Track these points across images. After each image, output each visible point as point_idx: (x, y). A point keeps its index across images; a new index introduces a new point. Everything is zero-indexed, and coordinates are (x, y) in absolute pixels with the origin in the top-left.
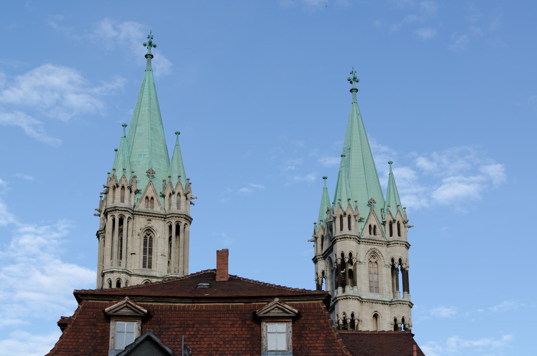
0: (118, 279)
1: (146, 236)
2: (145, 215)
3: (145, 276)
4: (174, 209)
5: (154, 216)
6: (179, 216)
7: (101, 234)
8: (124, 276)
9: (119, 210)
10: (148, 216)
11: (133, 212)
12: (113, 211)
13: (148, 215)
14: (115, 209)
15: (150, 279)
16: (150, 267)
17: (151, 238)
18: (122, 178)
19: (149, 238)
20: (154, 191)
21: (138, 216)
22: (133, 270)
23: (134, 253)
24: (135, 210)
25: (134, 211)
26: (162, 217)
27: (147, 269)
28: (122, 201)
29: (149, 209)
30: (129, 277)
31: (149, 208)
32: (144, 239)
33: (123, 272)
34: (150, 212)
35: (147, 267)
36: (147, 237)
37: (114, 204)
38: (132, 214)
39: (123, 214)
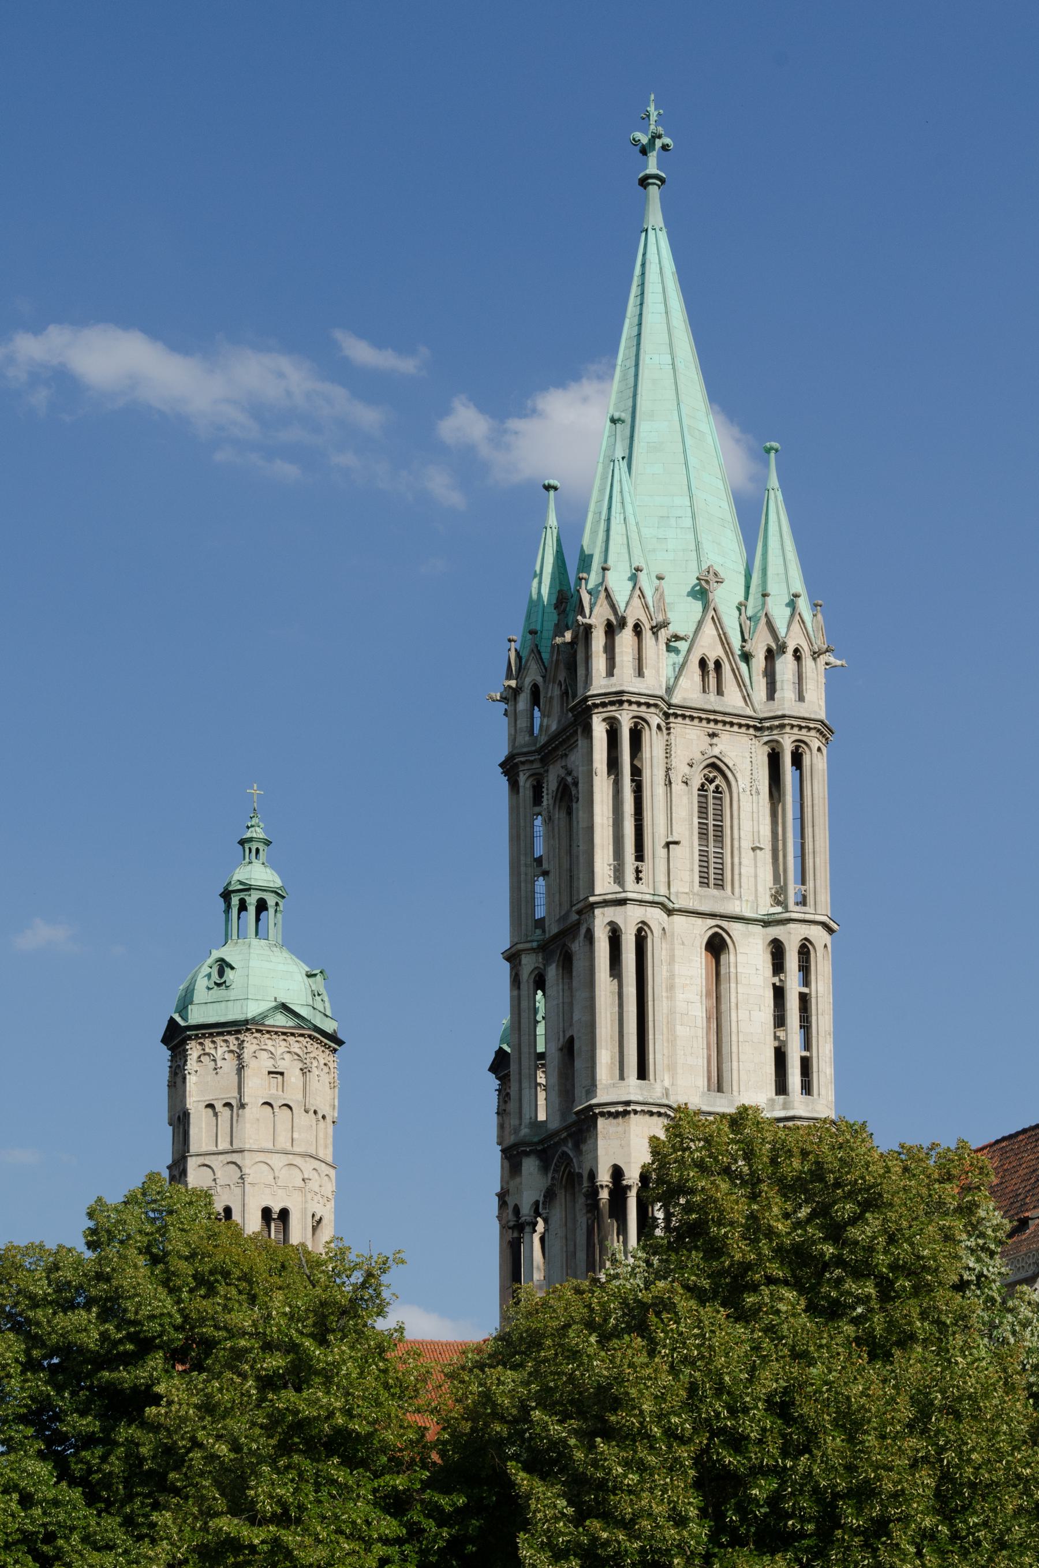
0: (640, 925)
1: (703, 785)
2: (701, 719)
3: (713, 916)
4: (786, 701)
5: (725, 723)
6: (804, 723)
7: (523, 763)
8: (658, 917)
9: (630, 703)
10: (709, 721)
11: (669, 709)
12: (612, 703)
13: (712, 717)
14: (618, 698)
15: (726, 923)
16: (720, 885)
17: (717, 790)
18: (631, 596)
19: (714, 792)
20: (724, 640)
21: (680, 720)
22: (677, 893)
23: (677, 840)
24: (675, 701)
25: (670, 705)
26: (748, 727)
27: (713, 891)
28: (640, 673)
29: (712, 696)
30: (665, 916)
31: (711, 694)
32: (699, 795)
33: (653, 903)
34: (717, 709)
35: (712, 882)
36: (706, 788)
37: (613, 680)
38: (667, 715)
39: (643, 715)
